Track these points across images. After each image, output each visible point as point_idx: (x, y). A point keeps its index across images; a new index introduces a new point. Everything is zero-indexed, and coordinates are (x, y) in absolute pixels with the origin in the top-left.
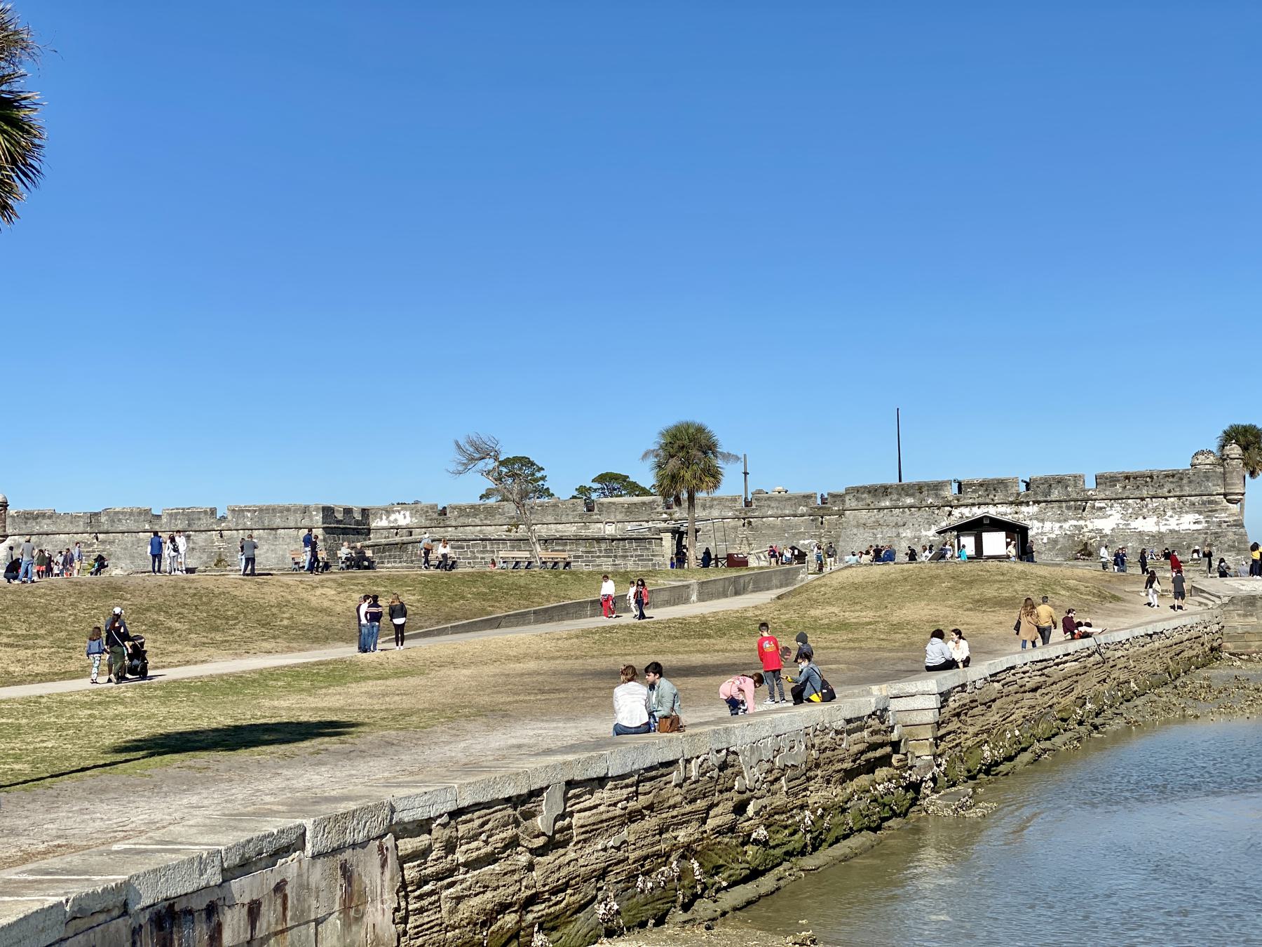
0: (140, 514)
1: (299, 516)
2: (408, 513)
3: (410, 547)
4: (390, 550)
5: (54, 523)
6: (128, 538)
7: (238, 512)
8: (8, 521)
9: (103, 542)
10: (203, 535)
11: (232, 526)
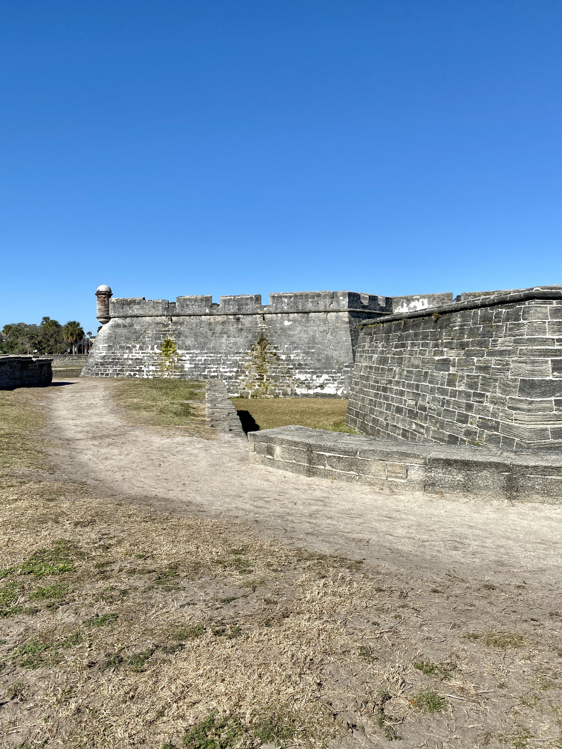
0: (202, 300)
1: (328, 301)
2: (426, 301)
3: (458, 319)
4: (416, 326)
5: (142, 308)
6: (194, 320)
7: (277, 298)
8: (111, 306)
9: (175, 323)
10: (250, 318)
11: (272, 310)
